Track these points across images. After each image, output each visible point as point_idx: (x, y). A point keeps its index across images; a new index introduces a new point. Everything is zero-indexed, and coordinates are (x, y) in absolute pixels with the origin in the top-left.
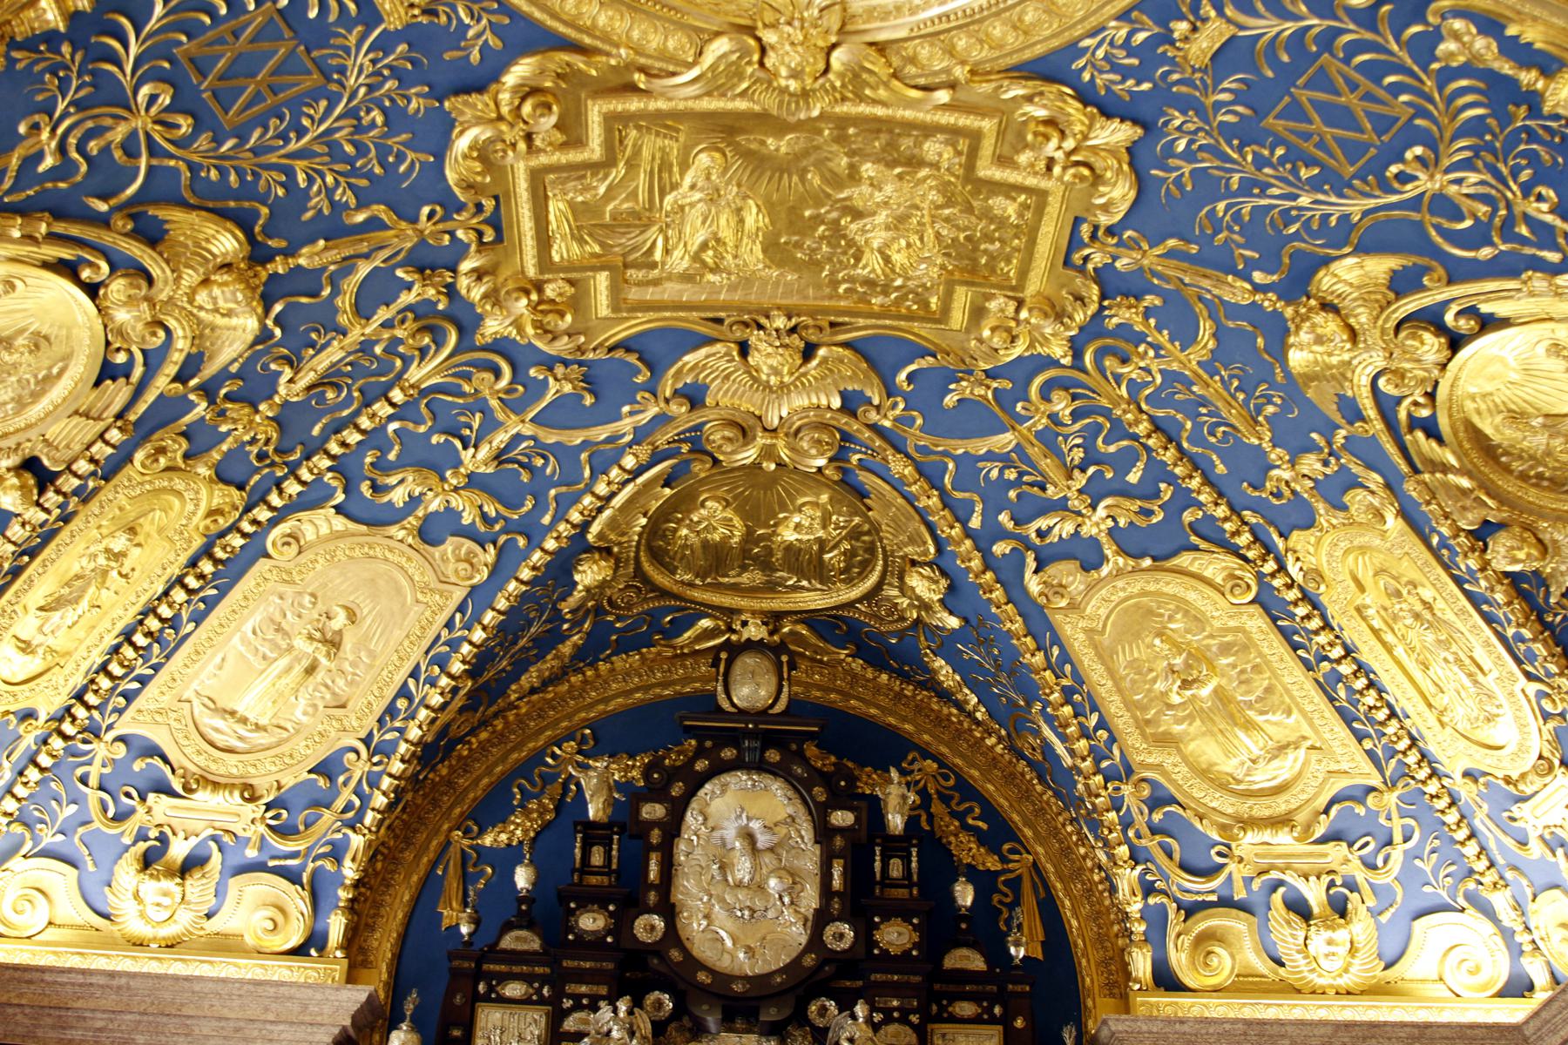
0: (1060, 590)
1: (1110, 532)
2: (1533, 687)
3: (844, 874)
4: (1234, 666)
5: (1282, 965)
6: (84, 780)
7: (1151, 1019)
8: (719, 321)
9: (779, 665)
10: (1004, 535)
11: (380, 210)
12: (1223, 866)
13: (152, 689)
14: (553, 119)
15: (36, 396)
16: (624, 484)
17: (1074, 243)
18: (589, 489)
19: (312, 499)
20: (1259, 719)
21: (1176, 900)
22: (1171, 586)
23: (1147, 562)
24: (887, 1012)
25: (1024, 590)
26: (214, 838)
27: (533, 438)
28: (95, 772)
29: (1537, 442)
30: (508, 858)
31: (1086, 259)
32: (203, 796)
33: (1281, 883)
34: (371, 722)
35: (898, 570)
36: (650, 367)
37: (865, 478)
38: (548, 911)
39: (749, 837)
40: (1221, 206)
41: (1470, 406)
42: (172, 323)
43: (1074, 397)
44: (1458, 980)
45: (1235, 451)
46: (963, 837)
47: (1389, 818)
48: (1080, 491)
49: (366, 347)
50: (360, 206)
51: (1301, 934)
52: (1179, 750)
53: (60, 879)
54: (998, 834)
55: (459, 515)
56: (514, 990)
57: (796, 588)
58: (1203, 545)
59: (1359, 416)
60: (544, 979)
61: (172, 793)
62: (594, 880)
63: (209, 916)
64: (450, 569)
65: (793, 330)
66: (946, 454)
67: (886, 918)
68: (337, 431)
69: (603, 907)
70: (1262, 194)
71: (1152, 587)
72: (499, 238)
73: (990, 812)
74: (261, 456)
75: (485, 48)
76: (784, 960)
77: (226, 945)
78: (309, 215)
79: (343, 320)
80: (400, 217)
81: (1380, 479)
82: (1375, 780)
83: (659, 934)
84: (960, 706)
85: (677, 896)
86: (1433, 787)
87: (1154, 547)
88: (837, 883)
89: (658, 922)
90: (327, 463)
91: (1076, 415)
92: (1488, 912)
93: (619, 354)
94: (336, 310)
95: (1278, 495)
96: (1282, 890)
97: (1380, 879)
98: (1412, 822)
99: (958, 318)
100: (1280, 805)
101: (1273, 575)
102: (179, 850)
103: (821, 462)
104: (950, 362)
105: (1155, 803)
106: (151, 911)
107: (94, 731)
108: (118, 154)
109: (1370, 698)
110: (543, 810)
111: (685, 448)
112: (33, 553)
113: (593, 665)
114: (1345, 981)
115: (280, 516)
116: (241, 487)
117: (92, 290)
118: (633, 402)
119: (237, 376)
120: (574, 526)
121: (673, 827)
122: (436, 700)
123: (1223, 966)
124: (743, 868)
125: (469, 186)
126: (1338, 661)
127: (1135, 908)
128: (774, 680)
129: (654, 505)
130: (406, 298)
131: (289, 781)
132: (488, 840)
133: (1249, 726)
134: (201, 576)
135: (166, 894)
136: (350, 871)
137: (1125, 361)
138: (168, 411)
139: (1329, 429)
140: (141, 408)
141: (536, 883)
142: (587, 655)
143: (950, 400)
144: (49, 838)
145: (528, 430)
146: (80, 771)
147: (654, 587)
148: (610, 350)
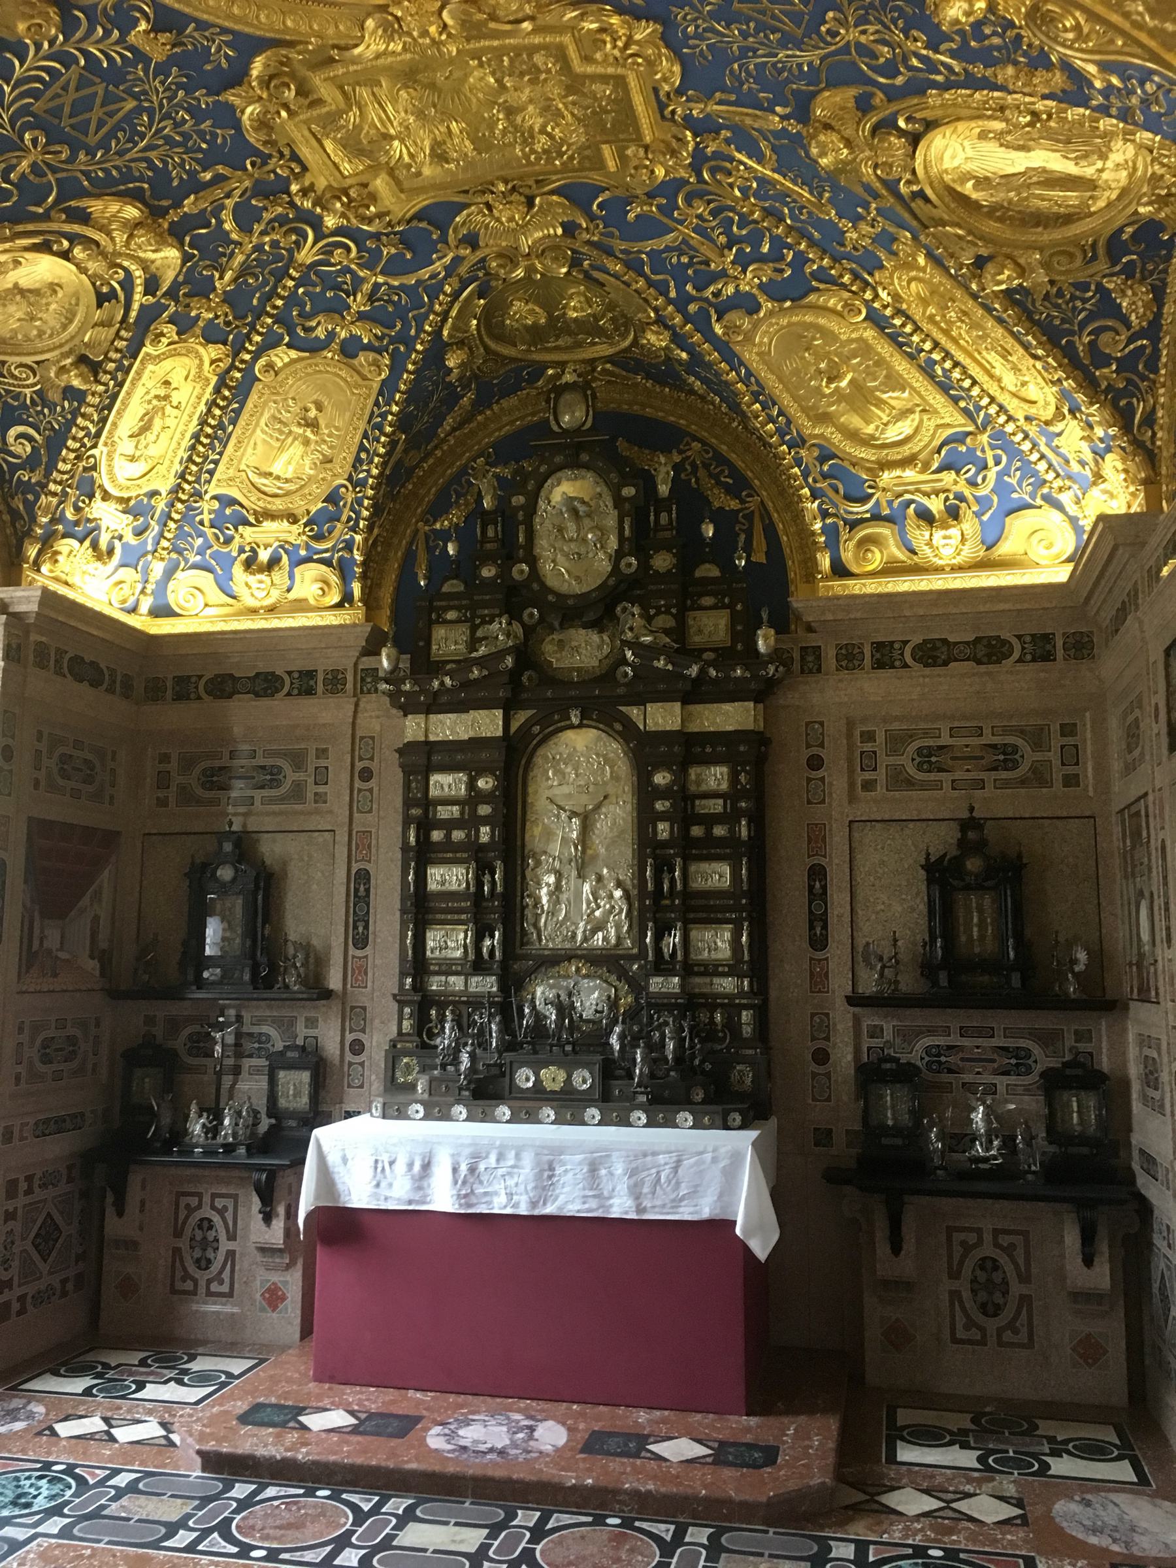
0: (737, 329)
1: (761, 286)
2: (1039, 365)
3: (631, 527)
4: (860, 364)
5: (914, 552)
6: (201, 523)
7: (829, 599)
8: (466, 192)
9: (586, 396)
10: (692, 299)
11: (220, 169)
12: (872, 495)
13: (221, 467)
14: (293, 93)
15: (71, 321)
16: (452, 303)
17: (662, 107)
18: (431, 310)
19: (271, 343)
20: (885, 396)
21: (844, 520)
22: (808, 318)
23: (788, 304)
24: (658, 608)
25: (715, 334)
26: (281, 547)
27: (386, 283)
28: (206, 517)
29: (1000, 196)
30: (445, 536)
31: (673, 112)
32: (268, 525)
33: (913, 501)
34: (348, 468)
35: (642, 328)
36: (438, 228)
37: (596, 274)
38: (465, 568)
39: (575, 512)
40: (736, 66)
41: (947, 178)
42: (126, 264)
43: (709, 202)
44: (1037, 553)
45: (819, 224)
46: (716, 491)
47: (983, 451)
48: (733, 263)
49: (258, 248)
50: (204, 171)
51: (927, 534)
52: (834, 425)
53: (206, 580)
54: (739, 486)
55: (360, 338)
56: (451, 615)
57: (593, 344)
58: (822, 286)
59: (876, 196)
60: (467, 608)
61: (251, 525)
62: (489, 546)
63: (289, 590)
64: (365, 372)
65: (514, 189)
66: (640, 252)
67: (656, 552)
68: (269, 299)
69: (495, 562)
70: (755, 56)
71: (795, 319)
72: (305, 169)
73: (734, 472)
74: (228, 324)
75: (226, 56)
76: (599, 582)
77: (301, 606)
78: (175, 183)
79: (234, 236)
80: (235, 169)
81: (908, 235)
82: (971, 429)
83: (526, 575)
84: (713, 403)
85: (537, 551)
86: (1010, 428)
87: (793, 290)
88: (627, 533)
89: (525, 567)
90: (269, 321)
91: (715, 213)
92: (1059, 506)
93: (414, 223)
94: (227, 233)
95: (855, 248)
96: (913, 506)
97: (983, 492)
98: (999, 452)
99: (611, 165)
100: (906, 450)
101: (873, 301)
102: (264, 556)
103: (564, 270)
104: (619, 193)
105: (822, 459)
106: (256, 593)
107: (198, 495)
108: (31, 177)
109: (956, 374)
110: (467, 504)
111: (481, 274)
112: (109, 408)
113: (490, 407)
114: (957, 561)
115: (256, 356)
116: (225, 343)
117: (65, 255)
118: (437, 251)
119: (185, 282)
120: (429, 334)
121: (531, 509)
122: (382, 450)
123: (876, 559)
124: (571, 530)
125: (265, 143)
126: (930, 352)
127: (818, 526)
128: (584, 408)
129: (478, 311)
130: (266, 216)
131: (313, 510)
132: (438, 526)
133: (880, 403)
134: (224, 398)
135: (261, 582)
136: (358, 557)
137: (729, 174)
138: (149, 315)
139: (866, 206)
140: (133, 314)
141: (459, 552)
142: (481, 404)
143: (631, 216)
144: (194, 558)
145: (380, 280)
146: (198, 519)
147: (506, 358)
148: (409, 222)
